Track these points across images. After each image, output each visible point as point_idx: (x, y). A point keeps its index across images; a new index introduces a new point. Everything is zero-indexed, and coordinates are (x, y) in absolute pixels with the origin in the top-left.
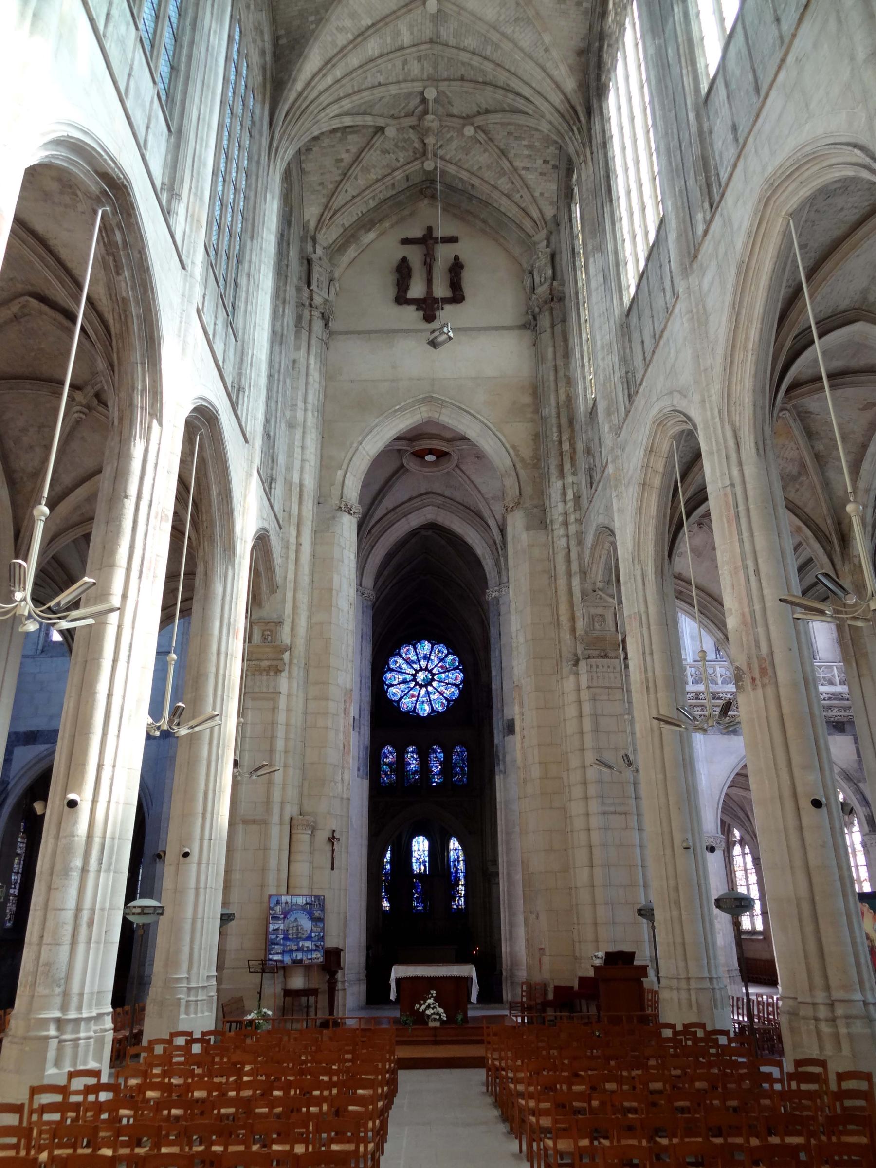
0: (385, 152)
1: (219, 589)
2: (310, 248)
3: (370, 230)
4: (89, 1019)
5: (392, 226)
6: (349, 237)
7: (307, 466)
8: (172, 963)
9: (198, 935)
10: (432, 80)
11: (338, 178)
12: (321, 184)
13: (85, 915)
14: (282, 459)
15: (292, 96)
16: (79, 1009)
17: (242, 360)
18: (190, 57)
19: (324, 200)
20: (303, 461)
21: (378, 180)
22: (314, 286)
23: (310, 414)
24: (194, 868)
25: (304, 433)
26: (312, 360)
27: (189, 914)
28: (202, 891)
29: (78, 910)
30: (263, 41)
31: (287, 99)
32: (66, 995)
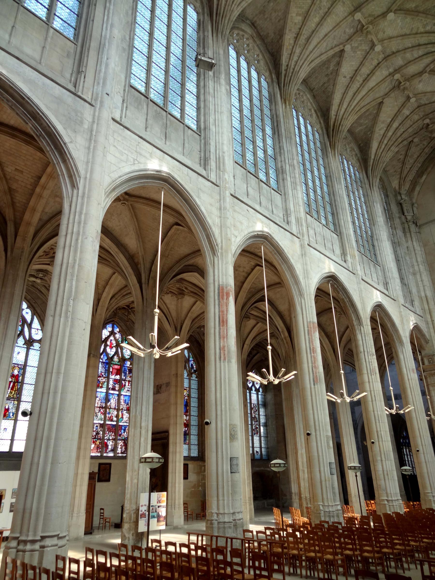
0: (417, 146)
1: (401, 357)
2: (399, 198)
3: (422, 176)
4: (395, 500)
5: (432, 168)
6: (414, 184)
7: (426, 288)
8: (425, 487)
9: (431, 478)
10: (426, 116)
11: (401, 166)
12: (395, 171)
13: (385, 472)
14: (414, 290)
15: (372, 161)
16: (392, 497)
17: (384, 272)
18: (336, 206)
19: (398, 176)
20: (424, 286)
21: (418, 157)
22: (406, 214)
23: (421, 266)
24: (422, 455)
25: (420, 274)
26: (415, 243)
27: (425, 470)
28: (427, 463)
29: (383, 471)
30: (355, 151)
31: (370, 165)
32: (387, 493)
